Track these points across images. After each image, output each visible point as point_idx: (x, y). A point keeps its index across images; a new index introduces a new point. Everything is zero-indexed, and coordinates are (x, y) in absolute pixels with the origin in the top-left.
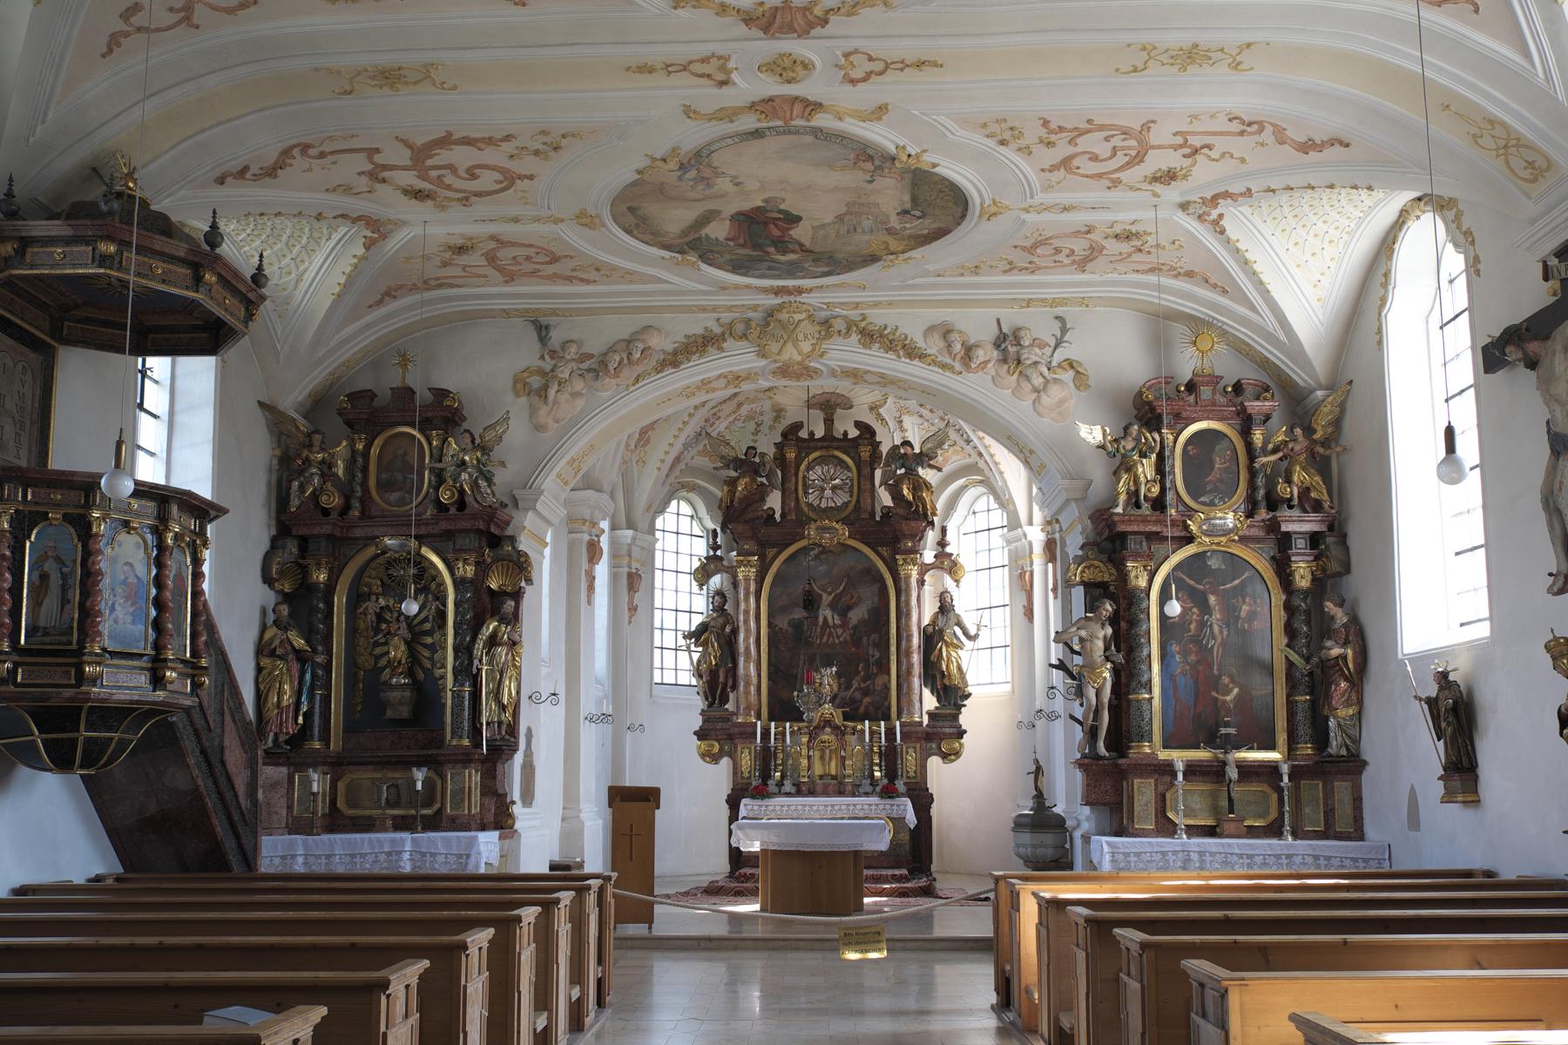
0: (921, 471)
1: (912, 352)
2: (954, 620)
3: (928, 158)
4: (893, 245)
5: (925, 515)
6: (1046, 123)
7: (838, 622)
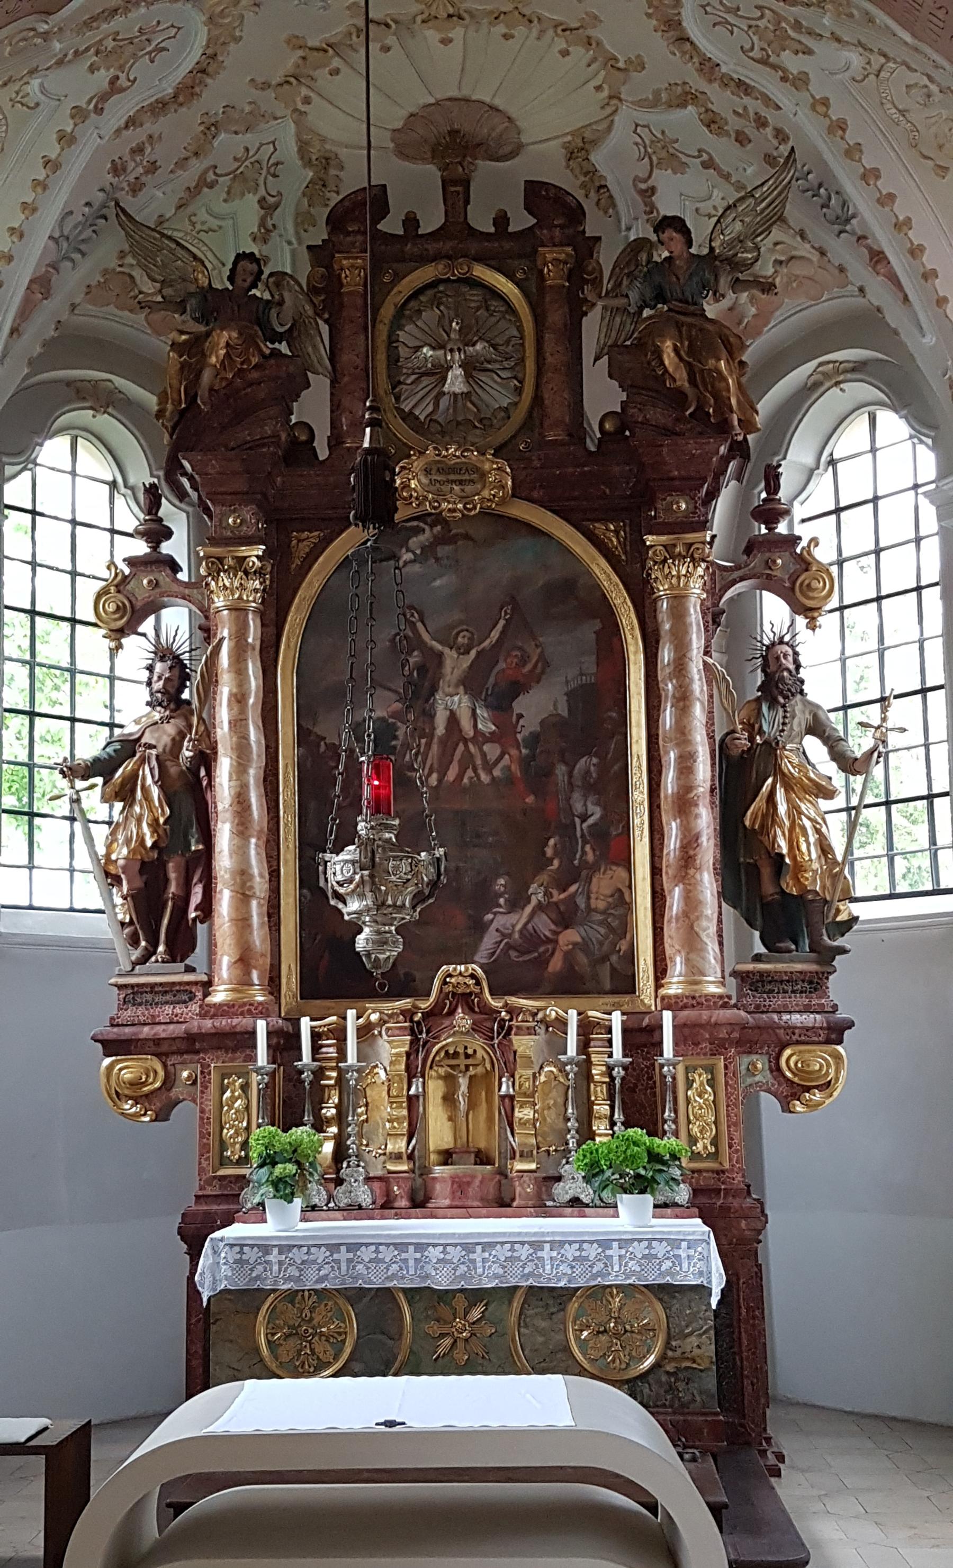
2: (801, 719)
5: (724, 428)
7: (487, 726)
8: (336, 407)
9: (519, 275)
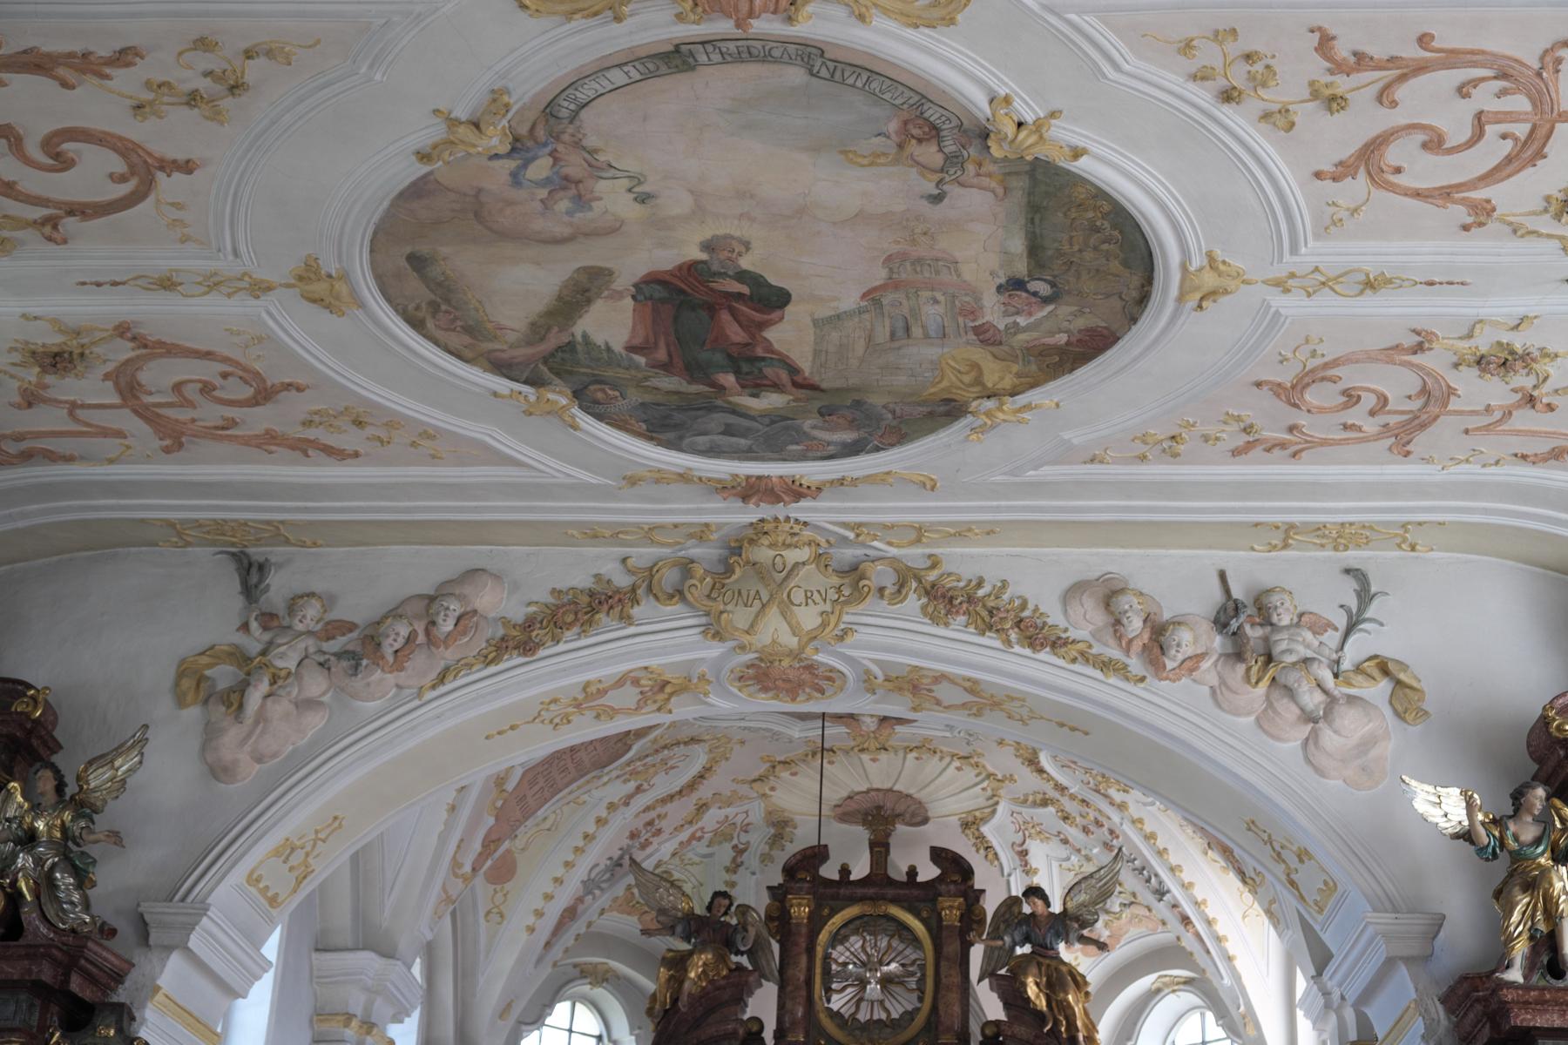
0: (1062, 947)
1: (1035, 634)
3: (1064, 133)
4: (994, 374)
6: (1325, 43)
8: (781, 1007)
9: (925, 914)
